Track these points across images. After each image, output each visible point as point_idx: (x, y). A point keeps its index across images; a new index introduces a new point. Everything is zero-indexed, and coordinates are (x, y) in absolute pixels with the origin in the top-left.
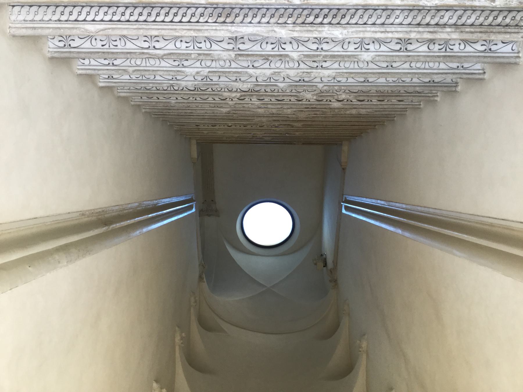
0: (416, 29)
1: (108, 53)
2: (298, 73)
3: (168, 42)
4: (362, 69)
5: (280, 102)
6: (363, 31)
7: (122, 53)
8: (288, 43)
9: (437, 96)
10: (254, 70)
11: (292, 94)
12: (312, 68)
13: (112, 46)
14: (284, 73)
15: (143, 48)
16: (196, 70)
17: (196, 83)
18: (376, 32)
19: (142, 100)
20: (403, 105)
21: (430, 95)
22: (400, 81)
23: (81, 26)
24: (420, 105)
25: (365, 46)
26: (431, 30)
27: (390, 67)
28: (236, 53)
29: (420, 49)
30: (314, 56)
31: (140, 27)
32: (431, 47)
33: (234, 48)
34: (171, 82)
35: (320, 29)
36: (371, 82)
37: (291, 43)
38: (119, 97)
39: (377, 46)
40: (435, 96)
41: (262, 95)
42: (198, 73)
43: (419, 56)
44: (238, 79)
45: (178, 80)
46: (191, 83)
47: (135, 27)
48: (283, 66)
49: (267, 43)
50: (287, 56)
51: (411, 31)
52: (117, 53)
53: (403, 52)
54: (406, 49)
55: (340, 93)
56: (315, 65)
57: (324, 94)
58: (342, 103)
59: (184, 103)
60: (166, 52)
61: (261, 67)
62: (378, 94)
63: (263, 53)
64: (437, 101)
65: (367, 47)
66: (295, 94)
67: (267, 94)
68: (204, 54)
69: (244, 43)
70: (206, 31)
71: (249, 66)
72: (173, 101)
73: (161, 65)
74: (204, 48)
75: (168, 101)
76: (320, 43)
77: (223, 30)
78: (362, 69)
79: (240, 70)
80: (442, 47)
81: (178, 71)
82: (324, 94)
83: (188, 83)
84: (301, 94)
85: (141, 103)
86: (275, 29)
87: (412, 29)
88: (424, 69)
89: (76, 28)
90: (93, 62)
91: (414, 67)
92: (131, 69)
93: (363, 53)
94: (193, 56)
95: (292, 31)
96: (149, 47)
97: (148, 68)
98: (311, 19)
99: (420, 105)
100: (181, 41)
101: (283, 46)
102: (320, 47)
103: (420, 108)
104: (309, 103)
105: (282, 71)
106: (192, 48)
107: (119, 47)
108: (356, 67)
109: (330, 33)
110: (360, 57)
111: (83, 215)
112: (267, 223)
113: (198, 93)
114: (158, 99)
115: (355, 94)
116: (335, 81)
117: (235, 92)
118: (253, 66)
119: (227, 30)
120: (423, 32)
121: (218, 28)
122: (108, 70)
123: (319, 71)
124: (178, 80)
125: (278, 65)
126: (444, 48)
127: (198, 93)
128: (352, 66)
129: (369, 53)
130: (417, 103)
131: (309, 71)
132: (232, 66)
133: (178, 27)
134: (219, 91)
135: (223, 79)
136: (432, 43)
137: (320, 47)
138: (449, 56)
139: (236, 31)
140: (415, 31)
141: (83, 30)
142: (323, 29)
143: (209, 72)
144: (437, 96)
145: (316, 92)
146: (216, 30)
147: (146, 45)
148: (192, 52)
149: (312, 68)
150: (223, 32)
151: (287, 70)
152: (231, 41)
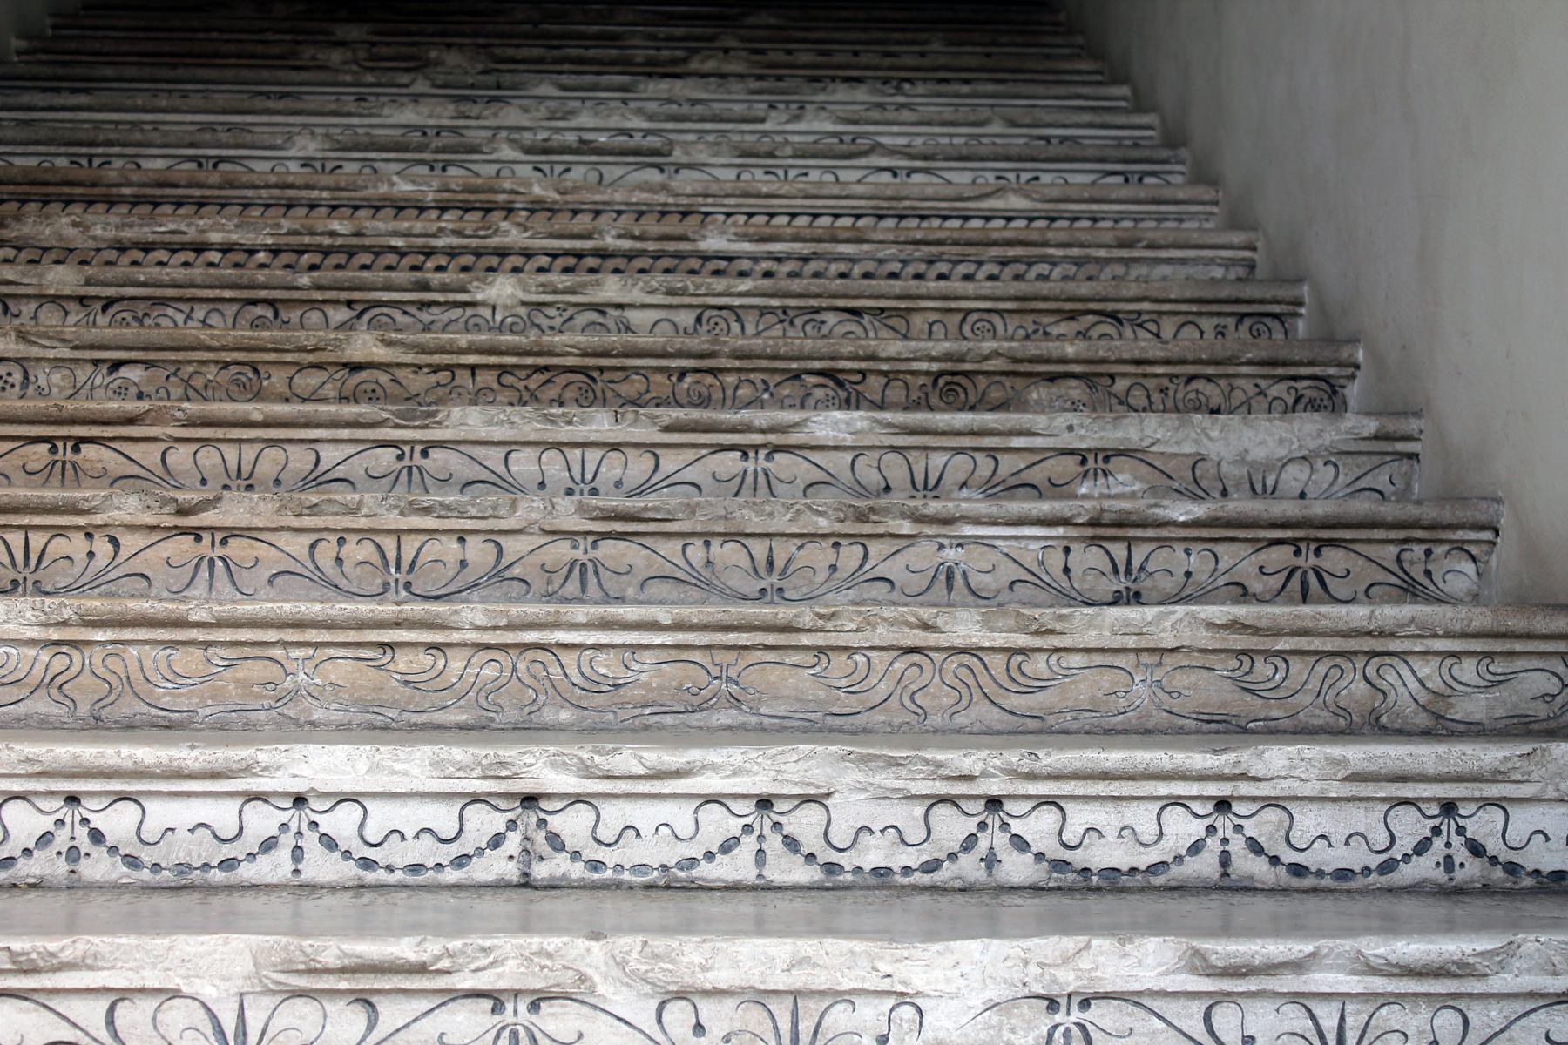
0: (208, 193)
7: (982, 159)
9: (19, 53)
10: (629, 125)
14: (539, 115)
15: (926, 171)
16: (801, 126)
17: (821, 97)
21: (44, 57)
23: (1039, 206)
24: (54, 27)
26: (168, 191)
28: (670, 159)
31: (894, 204)
35: (446, 195)
42: (796, 118)
46: (838, 97)
47: (907, 203)
50: (528, 150)
51: (220, 188)
52: (995, 160)
60: (863, 162)
63: (594, 158)
70: (729, 191)
77: (688, 196)
79: (670, 126)
81: (856, 122)
86: (558, 197)
87: (216, 192)
89: (1050, 201)
93: (319, 155)
94: (788, 151)
95: (518, 193)
97: (945, 130)
99: (54, 27)
115: (298, 63)
119: (678, 195)
121: (700, 200)
122: (1065, 126)
123: (432, 122)
129: (301, 154)
130: (65, 32)
131: (461, 122)
133: (799, 202)
138: (81, 144)
140: (211, 187)
143: (763, 121)
148: (791, 162)
151: (527, 124)
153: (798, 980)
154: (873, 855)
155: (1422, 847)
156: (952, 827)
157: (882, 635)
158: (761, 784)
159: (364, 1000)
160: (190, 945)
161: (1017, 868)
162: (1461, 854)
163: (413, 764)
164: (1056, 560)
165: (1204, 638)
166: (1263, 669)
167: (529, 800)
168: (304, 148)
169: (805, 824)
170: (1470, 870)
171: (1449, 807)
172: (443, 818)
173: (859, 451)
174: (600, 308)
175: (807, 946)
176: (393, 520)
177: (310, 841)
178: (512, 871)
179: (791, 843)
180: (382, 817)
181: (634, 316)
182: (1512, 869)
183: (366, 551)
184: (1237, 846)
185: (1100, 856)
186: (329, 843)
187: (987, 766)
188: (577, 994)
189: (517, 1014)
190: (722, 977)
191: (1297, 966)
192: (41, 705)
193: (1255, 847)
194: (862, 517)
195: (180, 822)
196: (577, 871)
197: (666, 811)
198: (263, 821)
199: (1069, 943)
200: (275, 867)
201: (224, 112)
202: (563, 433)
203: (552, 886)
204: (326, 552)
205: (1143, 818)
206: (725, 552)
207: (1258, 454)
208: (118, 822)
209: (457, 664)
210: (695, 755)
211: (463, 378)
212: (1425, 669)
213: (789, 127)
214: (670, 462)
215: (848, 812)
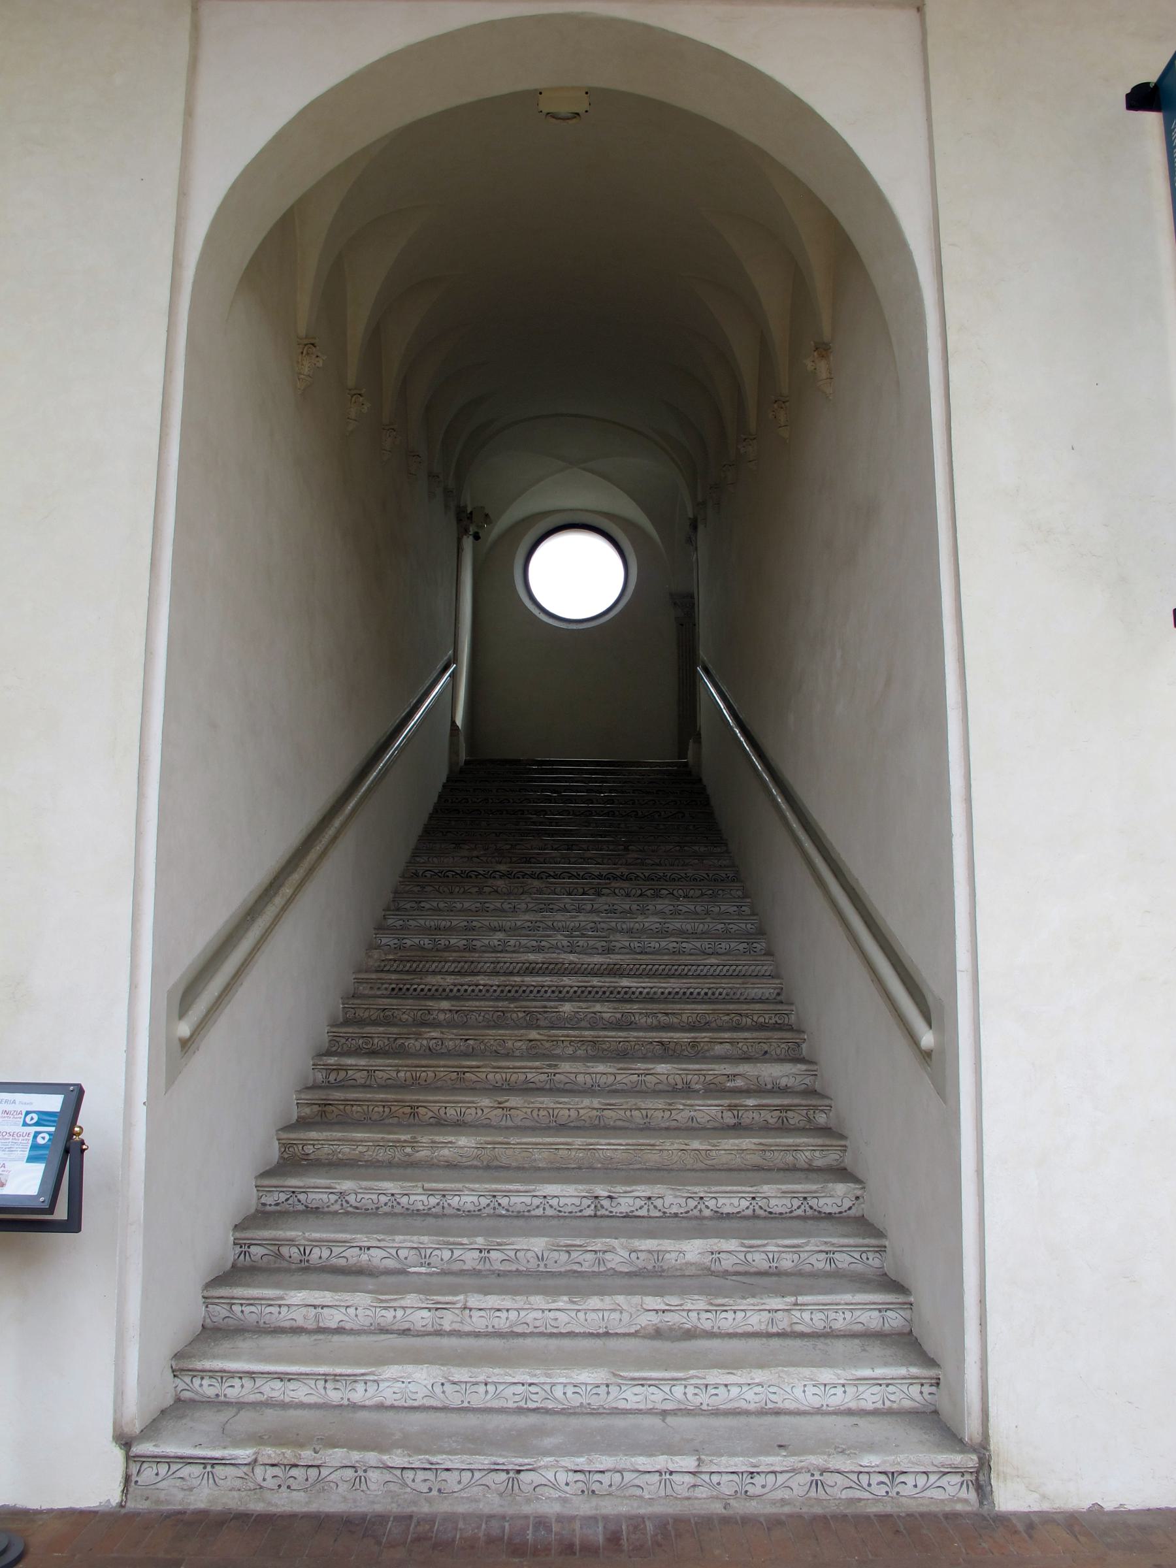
90: (743, 926)
98: (551, 966)
112: (577, 577)
135: (627, 907)
147: (684, 945)
153: (659, 1248)
154: (674, 1210)
155: (799, 1207)
156: (692, 1203)
157: (676, 1146)
158: (648, 1194)
159: (568, 1252)
160: (533, 1240)
161: (707, 1213)
162: (808, 1209)
163: (570, 1189)
164: (720, 1114)
165: (754, 1147)
166: (768, 1154)
167: (596, 1197)
169: (659, 1203)
170: (810, 1212)
171: (805, 1198)
172: (577, 1201)
173: (669, 1075)
174: (594, 1013)
175: (661, 1241)
176: (552, 1105)
177: (547, 1206)
178: (592, 1213)
179: (655, 1207)
180: (563, 1201)
181: (604, 1015)
182: (820, 1212)
183: (545, 1113)
184: (757, 1207)
185: (726, 1210)
186: (551, 1206)
187: (700, 1190)
188: (611, 1250)
189: (600, 1255)
190: (643, 1248)
191: (764, 1246)
192: (475, 1163)
193: (761, 1208)
194: (670, 1104)
195: (518, 1201)
196: (607, 1213)
197: (627, 1200)
198: (536, 1201)
199: (716, 1240)
200: (540, 1212)
202: (592, 1070)
203: (602, 1217)
204: (535, 1113)
205: (735, 1201)
206: (636, 1113)
207: (775, 1074)
208: (504, 1201)
209: (573, 1153)
210: (634, 1188)
211: (560, 1043)
212: (807, 1154)
214: (619, 1078)
215: (669, 1200)
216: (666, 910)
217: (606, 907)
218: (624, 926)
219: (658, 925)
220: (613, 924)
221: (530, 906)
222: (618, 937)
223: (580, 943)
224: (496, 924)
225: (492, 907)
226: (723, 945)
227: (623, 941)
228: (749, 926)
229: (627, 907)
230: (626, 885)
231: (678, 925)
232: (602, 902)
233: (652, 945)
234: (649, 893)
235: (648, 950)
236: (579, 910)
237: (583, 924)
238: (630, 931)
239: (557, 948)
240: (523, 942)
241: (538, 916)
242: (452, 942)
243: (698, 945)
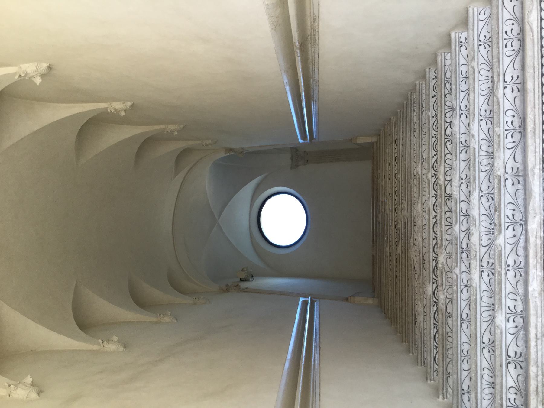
1: (498, 38)
2: (475, 245)
3: (512, 102)
4: (481, 315)
5: (431, 228)
6: (537, 314)
8: (514, 233)
9: (444, 398)
10: (477, 197)
11: (444, 240)
12: (481, 261)
13: (505, 41)
14: (474, 229)
16: (476, 135)
17: (458, 136)
18: (536, 328)
19: (431, 79)
20: (431, 362)
21: (445, 390)
22: (463, 358)
23: (535, 6)
24: (431, 380)
25: (512, 318)
27: (482, 346)
28: (502, 176)
29: (509, 378)
30: (500, 262)
31: (536, 70)
32: (512, 391)
33: (507, 173)
34: (458, 109)
36: (461, 326)
37: (515, 236)
38: (436, 55)
39: (512, 331)
40: (443, 396)
41: (441, 208)
43: (502, 376)
44: (462, 181)
45: (460, 116)
46: (457, 130)
47: (536, 63)
48: (482, 229)
49: (514, 210)
50: (500, 232)
51: (538, 366)
52: (499, 48)
53: (506, 359)
54: (509, 363)
55: (446, 293)
56: (485, 264)
57: (444, 275)
58: (432, 295)
59: (429, 124)
60: (501, 100)
61: (481, 205)
62: (444, 335)
63: (502, 206)
64: (438, 398)
65: (511, 320)
66: (444, 244)
67: (443, 214)
68: (500, 141)
69: (513, 184)
70: (533, 141)
71: (482, 191)
72: (430, 113)
73: (480, 97)
74: (507, 141)
75: (431, 108)
76: (514, 268)
77: (535, 159)
78: (481, 315)
80: (513, 402)
81: (474, 115)
82: (444, 275)
83: (459, 127)
84: (444, 251)
85: (427, 78)
88: (481, 384)
90: (481, 24)
91: (483, 372)
92: (475, 64)
95: (536, 235)
96: (506, 82)
97: (476, 83)
99: (431, 380)
100: (514, 116)
101: (511, 228)
102: (510, 268)
103: (427, 380)
104: (431, 260)
105: (477, 227)
106: (507, 128)
107: (505, 50)
108: (483, 309)
109: (534, 278)
110: (500, 312)
111: (315, 19)
113: (443, 139)
114: (433, 97)
115: (444, 309)
116: (462, 287)
117: (445, 179)
118: (482, 196)
120: (537, 380)
122: (474, 39)
124: (460, 116)
125: (484, 223)
126: (510, 405)
127: (443, 139)
128: (483, 304)
129: (504, 323)
130: (432, 377)
131: (478, 258)
132: (481, 173)
134: (445, 162)
135: (463, 164)
136: (516, 392)
137: (510, 268)
139: (534, 174)
141: (531, 8)
142: (539, 270)
143: (475, 149)
144: (444, 398)
145: (446, 266)
146: (535, 152)
147: (508, 78)
148: (502, 128)
149: (481, 261)
150: (533, 159)
151: (478, 234)
152: (515, 170)
168: (501, 321)
201: (476, 344)
213: (477, 139)
216: (466, 122)
217: (464, 186)
218: (485, 162)
219: (483, 123)
220: (483, 175)
221: (464, 268)
222: (499, 164)
223: (510, 213)
224: (485, 314)
225: (466, 311)
226: (508, 28)
227: (505, 160)
228: (482, 17)
229: (463, 164)
230: (442, 170)
231: (482, 99)
232: (457, 190)
233: (509, 119)
234: (449, 147)
235: (517, 123)
236: (467, 216)
237: (483, 211)
238: (491, 155)
239: (517, 243)
240: (509, 288)
241: (475, 264)
242: (511, 383)
243: (507, 60)
